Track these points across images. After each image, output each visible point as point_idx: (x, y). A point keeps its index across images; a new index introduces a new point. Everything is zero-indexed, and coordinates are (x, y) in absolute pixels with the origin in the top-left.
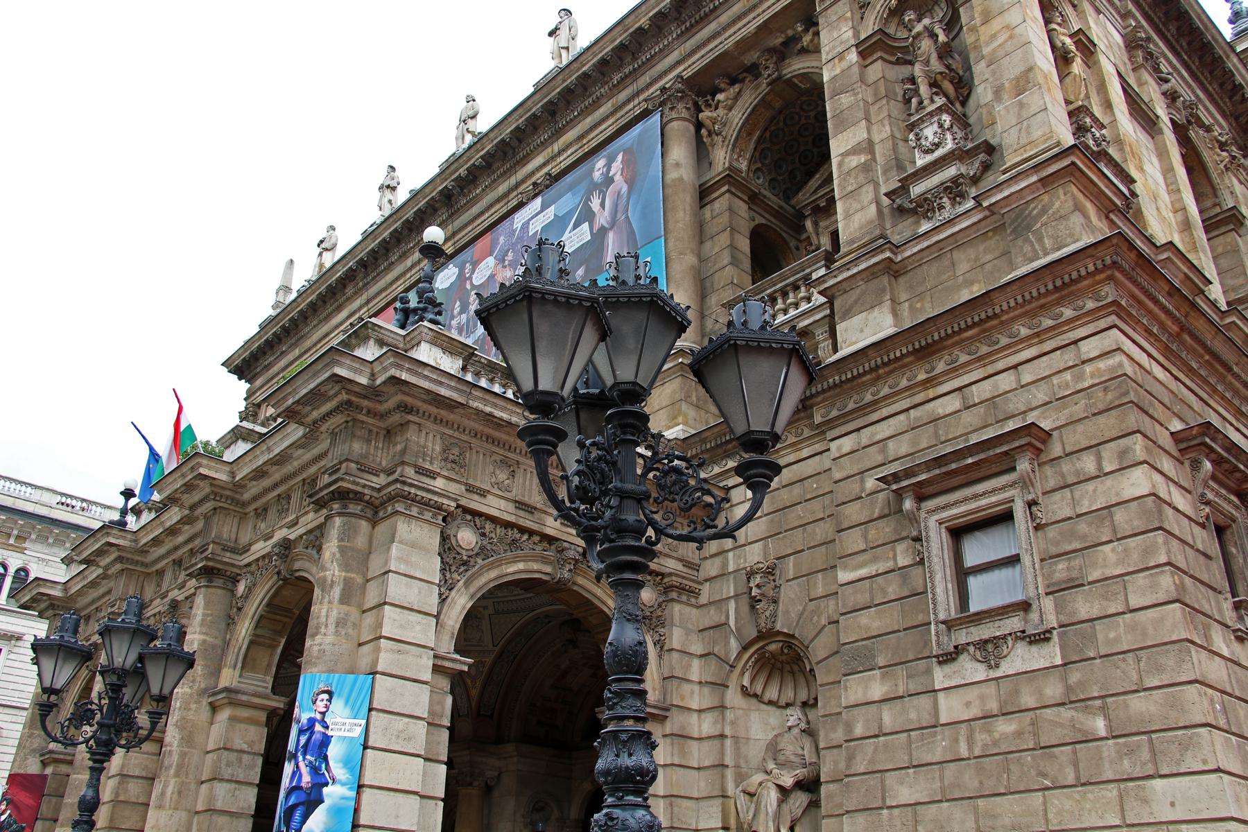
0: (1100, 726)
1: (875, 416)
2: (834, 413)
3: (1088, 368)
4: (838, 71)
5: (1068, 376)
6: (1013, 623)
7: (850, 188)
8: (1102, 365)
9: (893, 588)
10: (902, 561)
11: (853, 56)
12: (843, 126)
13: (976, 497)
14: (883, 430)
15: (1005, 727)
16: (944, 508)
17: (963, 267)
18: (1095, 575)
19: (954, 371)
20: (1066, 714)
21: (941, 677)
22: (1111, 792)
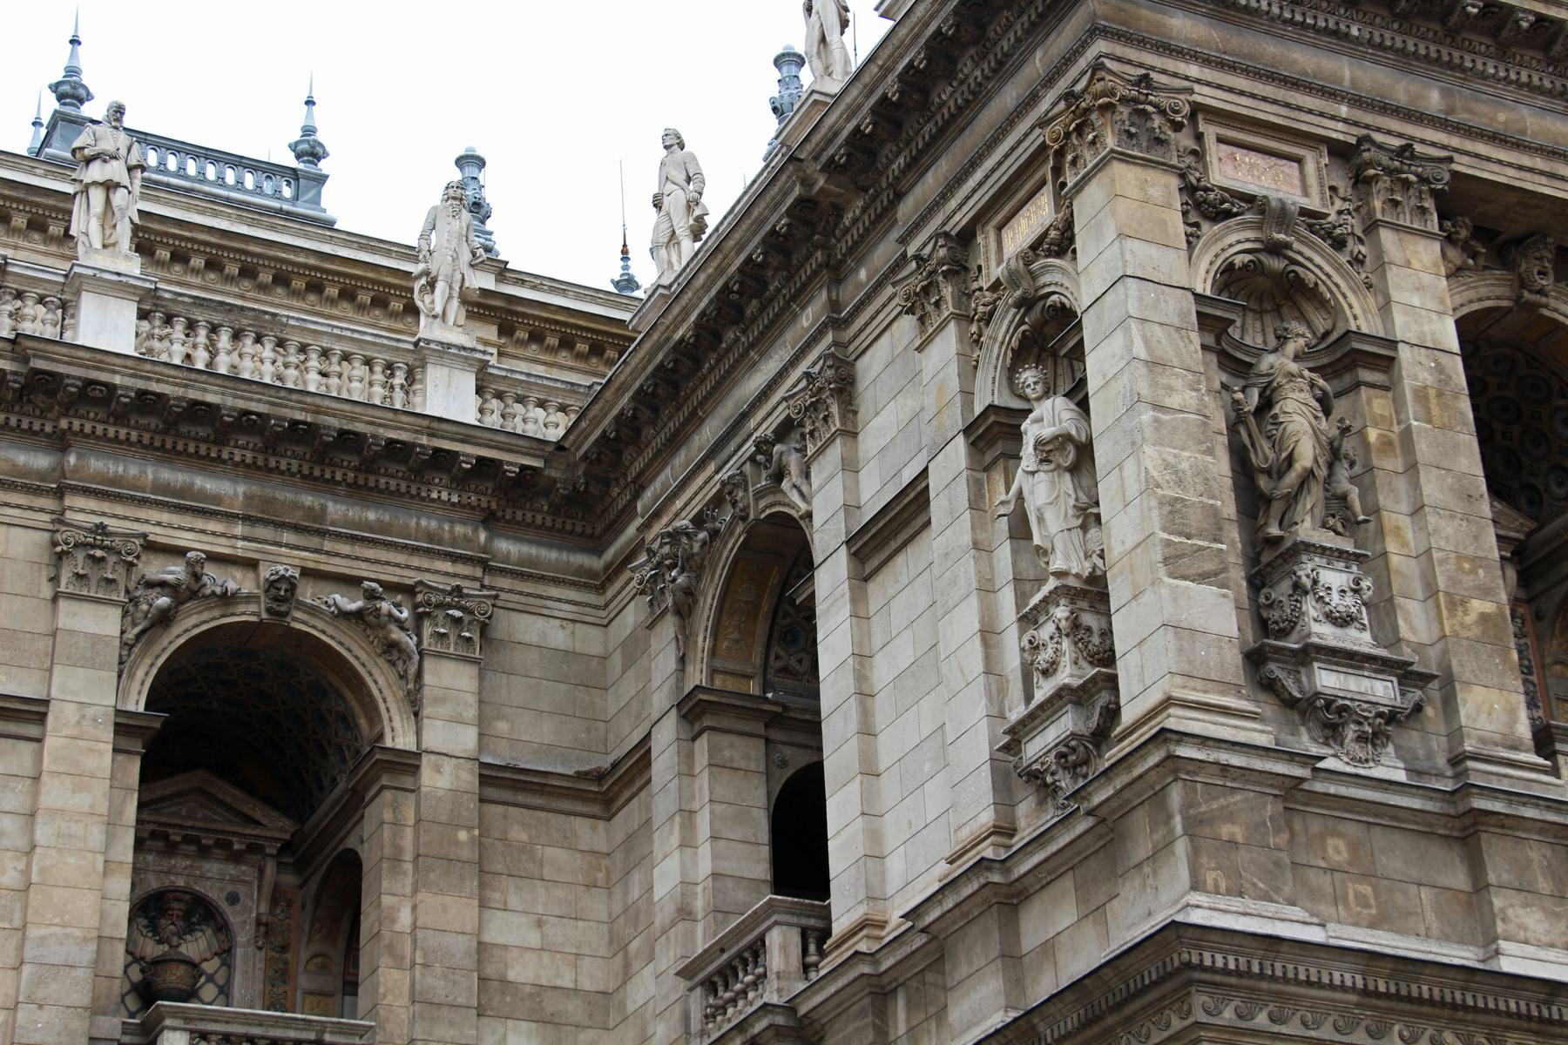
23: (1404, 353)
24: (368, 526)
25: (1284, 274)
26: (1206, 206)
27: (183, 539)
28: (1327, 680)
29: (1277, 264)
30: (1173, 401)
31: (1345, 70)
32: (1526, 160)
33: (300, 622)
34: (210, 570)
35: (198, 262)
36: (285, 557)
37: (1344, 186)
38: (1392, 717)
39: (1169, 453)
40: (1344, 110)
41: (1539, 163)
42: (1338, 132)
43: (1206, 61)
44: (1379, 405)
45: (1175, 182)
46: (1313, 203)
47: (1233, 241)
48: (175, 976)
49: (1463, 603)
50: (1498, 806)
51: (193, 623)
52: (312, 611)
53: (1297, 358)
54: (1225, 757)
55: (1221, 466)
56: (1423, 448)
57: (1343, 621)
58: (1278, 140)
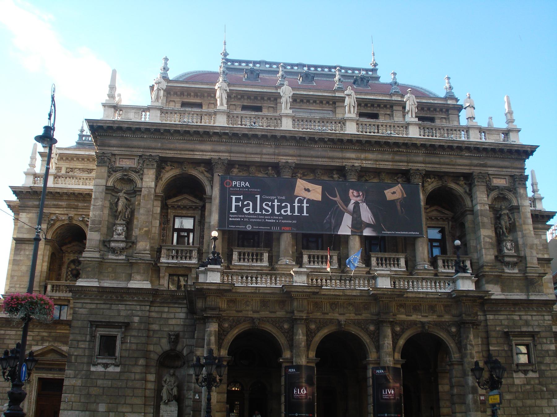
0: (545, 389)
1: (500, 313)
2: (490, 309)
3: (546, 322)
4: (483, 209)
5: (542, 322)
6: (530, 368)
7: (487, 247)
8: (549, 322)
9: (504, 354)
10: (506, 349)
11: (487, 207)
12: (484, 227)
13: (524, 340)
14: (501, 317)
15: (528, 387)
16: (518, 340)
17: (515, 284)
18: (545, 362)
19: (520, 311)
20: (539, 386)
21: (515, 375)
22: (546, 401)
23: (143, 189)
24: (85, 206)
25: (128, 179)
26: (112, 170)
27: (57, 212)
28: (113, 244)
29: (126, 177)
30: (98, 204)
31: (142, 143)
32: (176, 152)
33: (74, 222)
34: (61, 216)
35: (86, 160)
36: (72, 213)
37: (141, 161)
38: (123, 249)
39: (94, 213)
40: (142, 150)
41: (179, 152)
42: (140, 154)
43: (117, 147)
44: (138, 197)
45: (107, 168)
46: (135, 166)
47: (119, 175)
48: (75, 272)
49: (142, 229)
50: (134, 261)
51: (58, 224)
52: (76, 221)
53: (124, 193)
54: (87, 259)
55: (106, 211)
56: (142, 204)
57: (119, 235)
58: (130, 157)
